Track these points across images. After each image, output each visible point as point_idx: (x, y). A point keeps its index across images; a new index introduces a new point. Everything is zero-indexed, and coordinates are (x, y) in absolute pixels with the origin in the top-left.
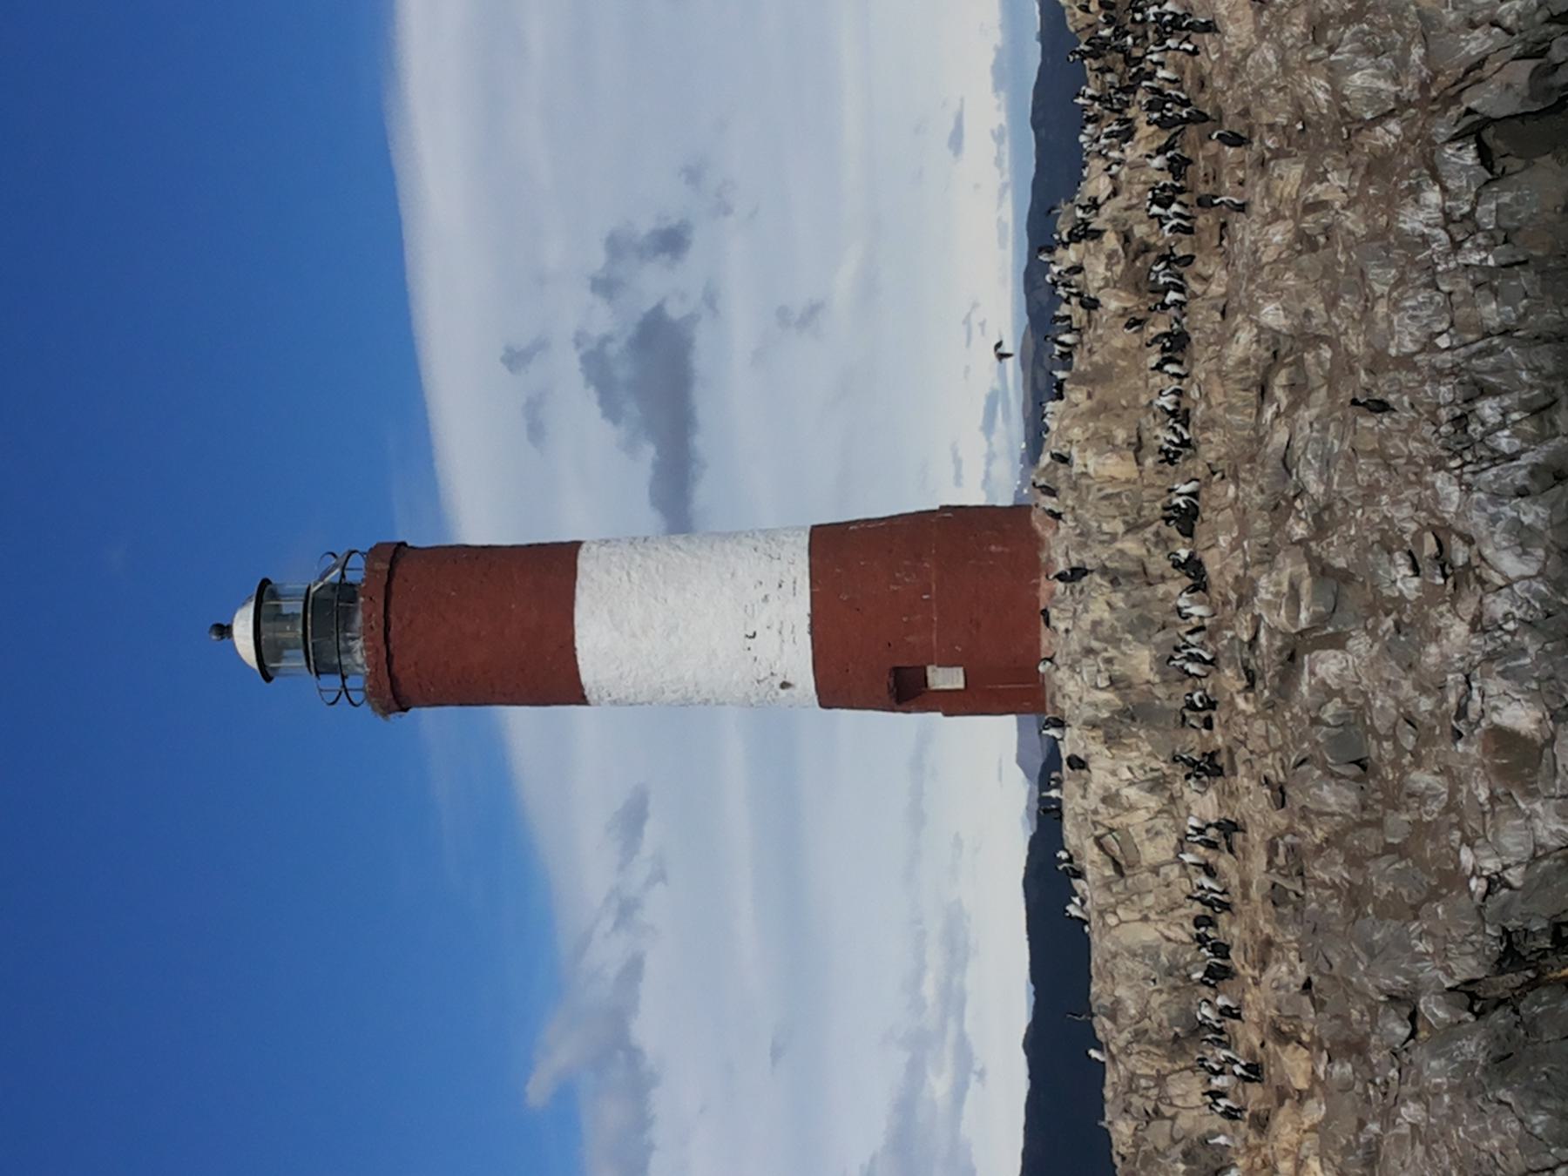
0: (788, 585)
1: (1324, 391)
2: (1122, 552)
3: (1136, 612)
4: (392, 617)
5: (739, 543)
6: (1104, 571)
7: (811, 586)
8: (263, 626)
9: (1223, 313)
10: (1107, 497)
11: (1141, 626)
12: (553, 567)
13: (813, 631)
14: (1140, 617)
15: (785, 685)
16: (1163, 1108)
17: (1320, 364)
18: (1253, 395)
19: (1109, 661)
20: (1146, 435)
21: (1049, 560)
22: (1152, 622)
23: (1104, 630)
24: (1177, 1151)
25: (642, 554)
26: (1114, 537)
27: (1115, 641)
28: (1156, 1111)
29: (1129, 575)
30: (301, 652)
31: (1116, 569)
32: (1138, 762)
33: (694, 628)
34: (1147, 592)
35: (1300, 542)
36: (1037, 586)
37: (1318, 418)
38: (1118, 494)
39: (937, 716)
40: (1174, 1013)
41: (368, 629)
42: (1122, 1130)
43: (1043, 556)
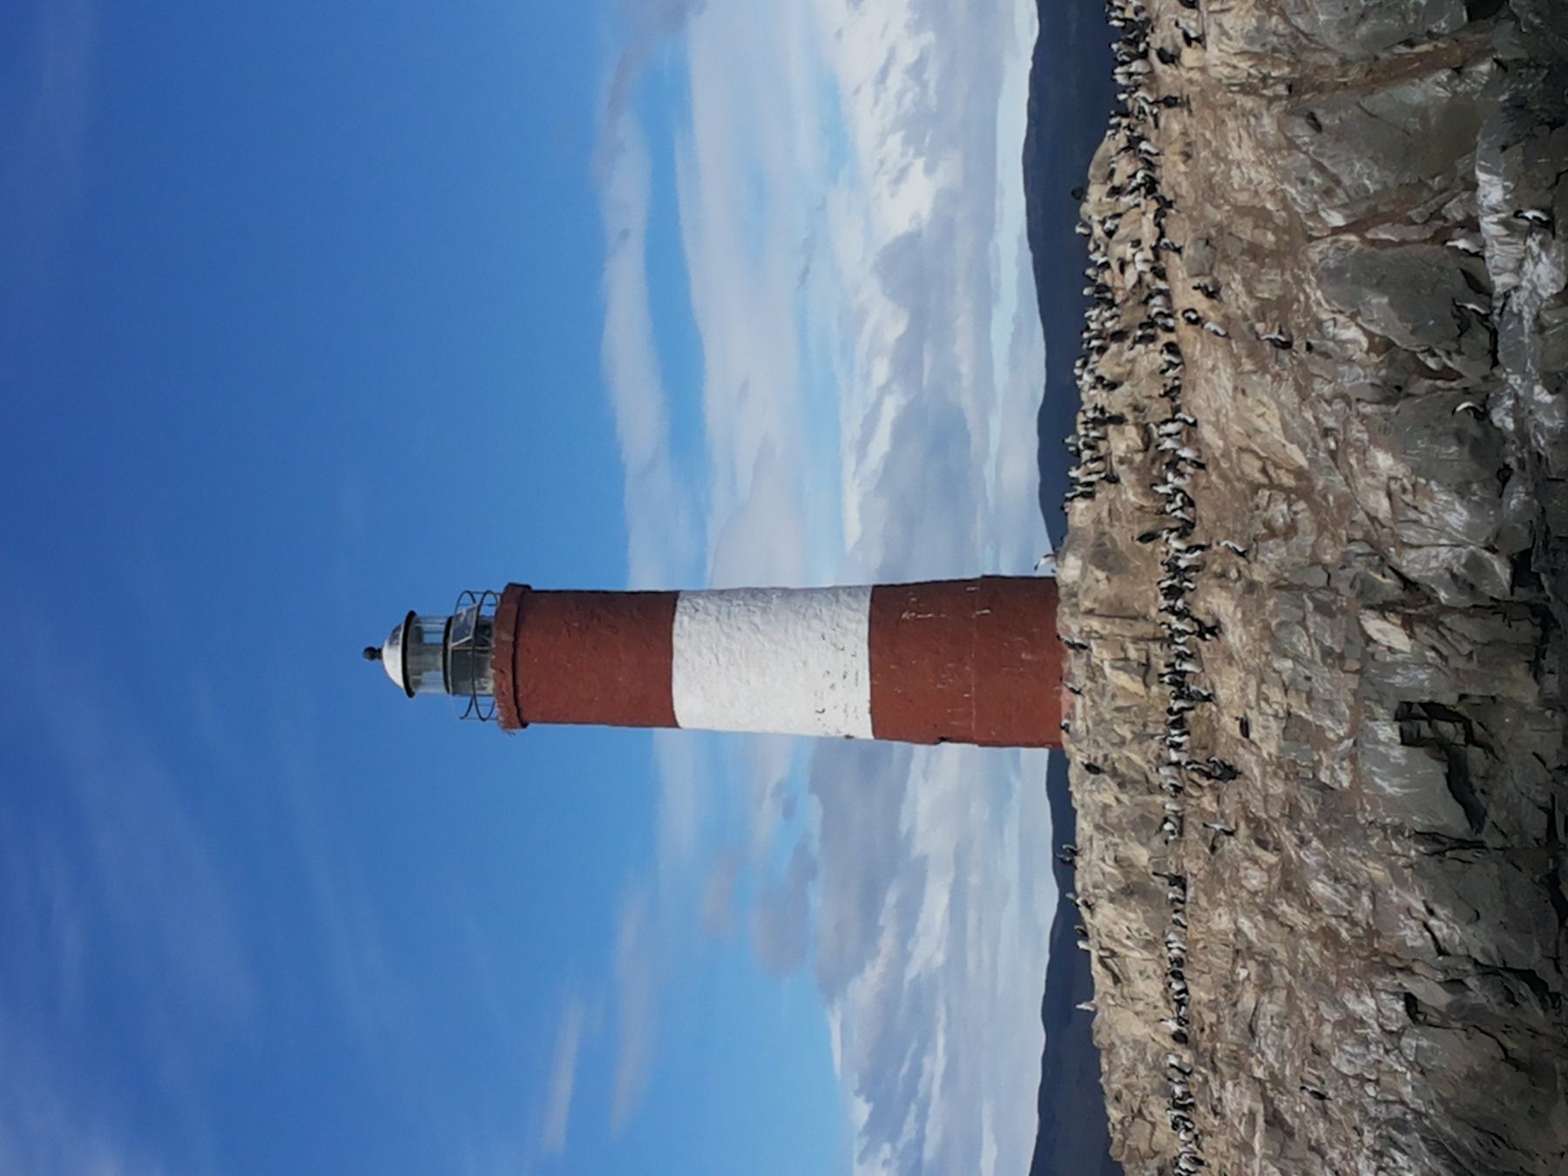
0: (851, 677)
1: (1283, 994)
2: (1128, 758)
3: (1139, 811)
4: (519, 682)
5: (809, 627)
6: (1114, 773)
7: (872, 678)
8: (409, 658)
9: (1213, 849)
10: (1118, 709)
11: (1145, 825)
12: (653, 614)
13: (871, 711)
14: (1142, 816)
15: (848, 737)
16: (1145, 1112)
17: (1282, 976)
18: (1229, 950)
19: (1116, 845)
20: (1153, 660)
21: (1070, 673)
22: (1150, 820)
23: (1113, 816)
24: (1153, 1164)
25: (728, 636)
26: (1123, 742)
27: (1119, 829)
28: (1140, 1111)
29: (1134, 782)
30: (441, 674)
31: (1123, 776)
32: (1134, 926)
33: (769, 687)
34: (1148, 798)
35: (1259, 1080)
36: (1059, 693)
37: (1278, 1015)
38: (1129, 708)
39: (976, 747)
40: (1155, 1085)
41: (498, 687)
42: (1114, 1114)
43: (1065, 666)
